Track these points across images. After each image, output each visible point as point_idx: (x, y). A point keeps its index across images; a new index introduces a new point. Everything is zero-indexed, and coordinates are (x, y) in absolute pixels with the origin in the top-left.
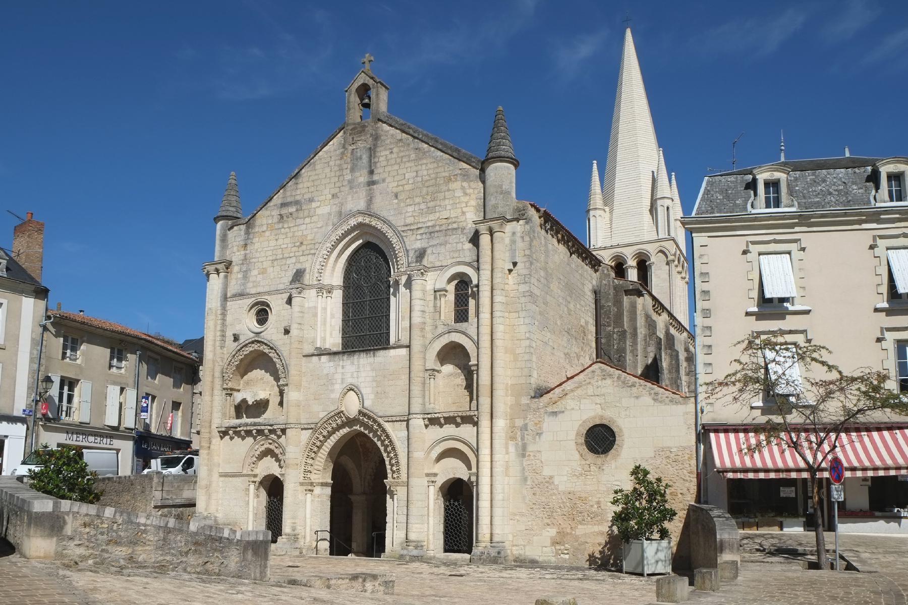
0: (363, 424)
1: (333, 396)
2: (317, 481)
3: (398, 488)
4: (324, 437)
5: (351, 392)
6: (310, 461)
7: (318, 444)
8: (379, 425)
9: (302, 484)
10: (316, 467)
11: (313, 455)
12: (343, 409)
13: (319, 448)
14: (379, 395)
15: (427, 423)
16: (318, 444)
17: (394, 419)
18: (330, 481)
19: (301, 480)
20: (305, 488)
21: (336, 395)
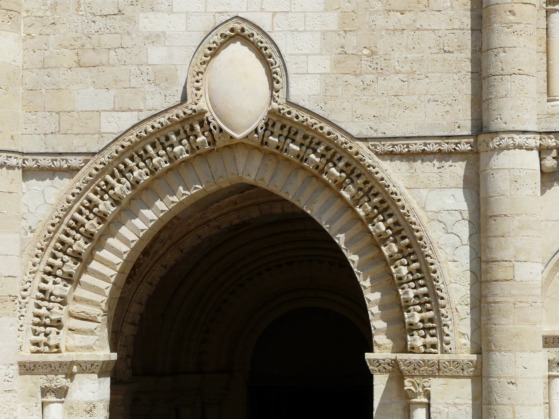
0: (276, 156)
1: (156, 55)
2: (86, 356)
3: (436, 385)
4: (116, 202)
5: (238, 50)
6: (59, 288)
7: (93, 225)
8: (355, 170)
9: (26, 368)
10: (73, 307)
11: (71, 267)
12: (203, 104)
13: (96, 241)
14: (357, 60)
15: (550, 162)
16: (93, 225)
17: (417, 146)
18: (105, 354)
19: (28, 355)
20: (41, 380)
21: (175, 55)
